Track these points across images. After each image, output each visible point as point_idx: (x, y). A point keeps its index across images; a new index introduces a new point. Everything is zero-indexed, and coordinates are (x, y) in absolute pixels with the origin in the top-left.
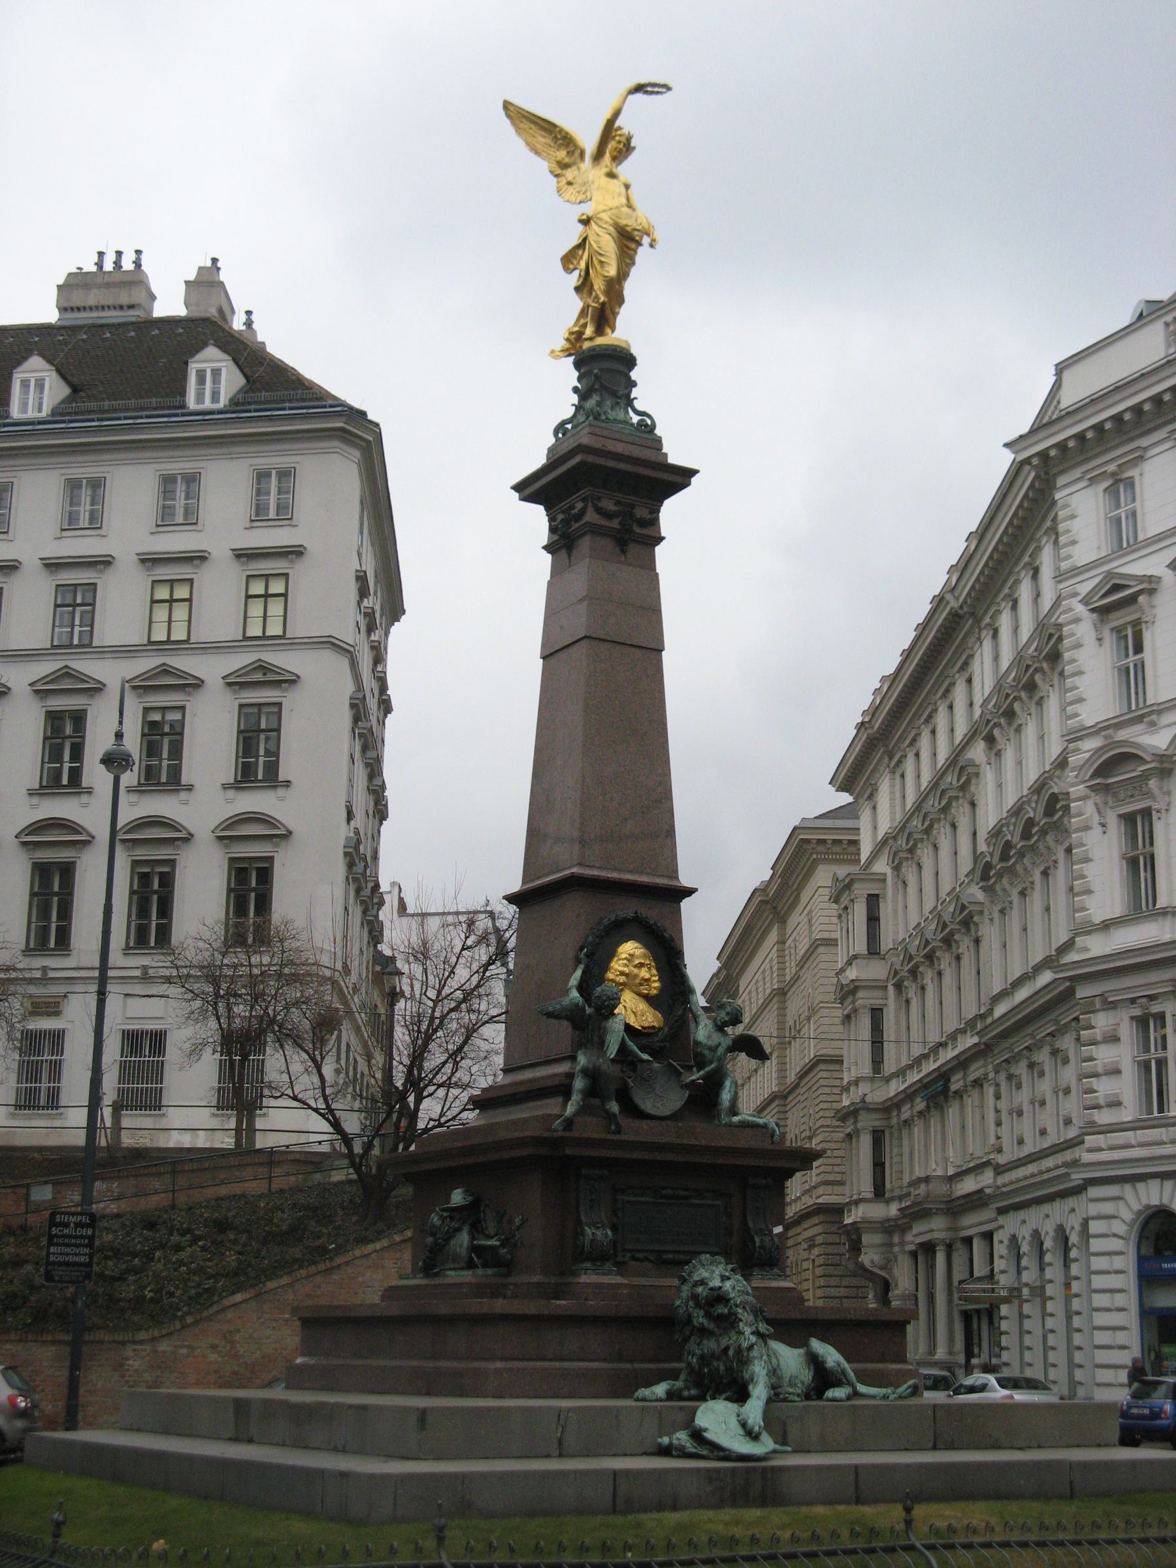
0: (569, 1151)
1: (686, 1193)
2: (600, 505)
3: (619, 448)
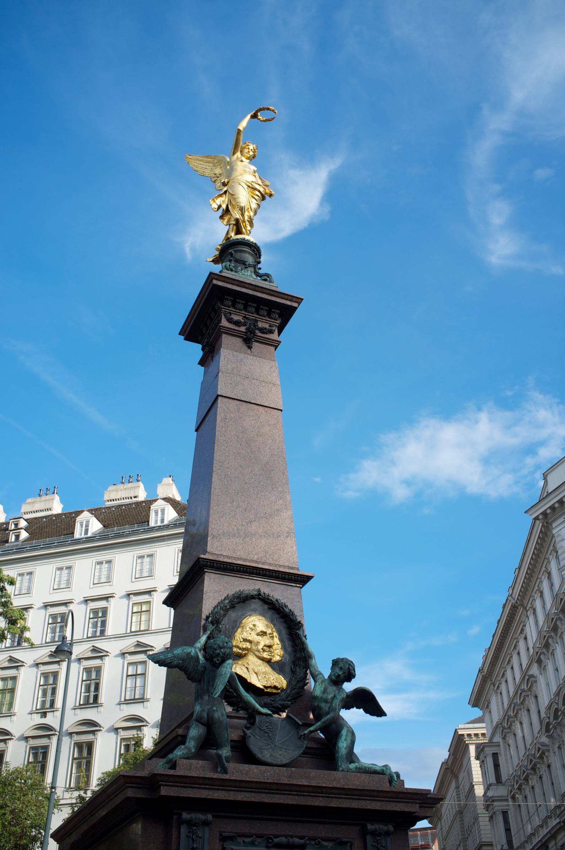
0: (164, 791)
1: (302, 841)
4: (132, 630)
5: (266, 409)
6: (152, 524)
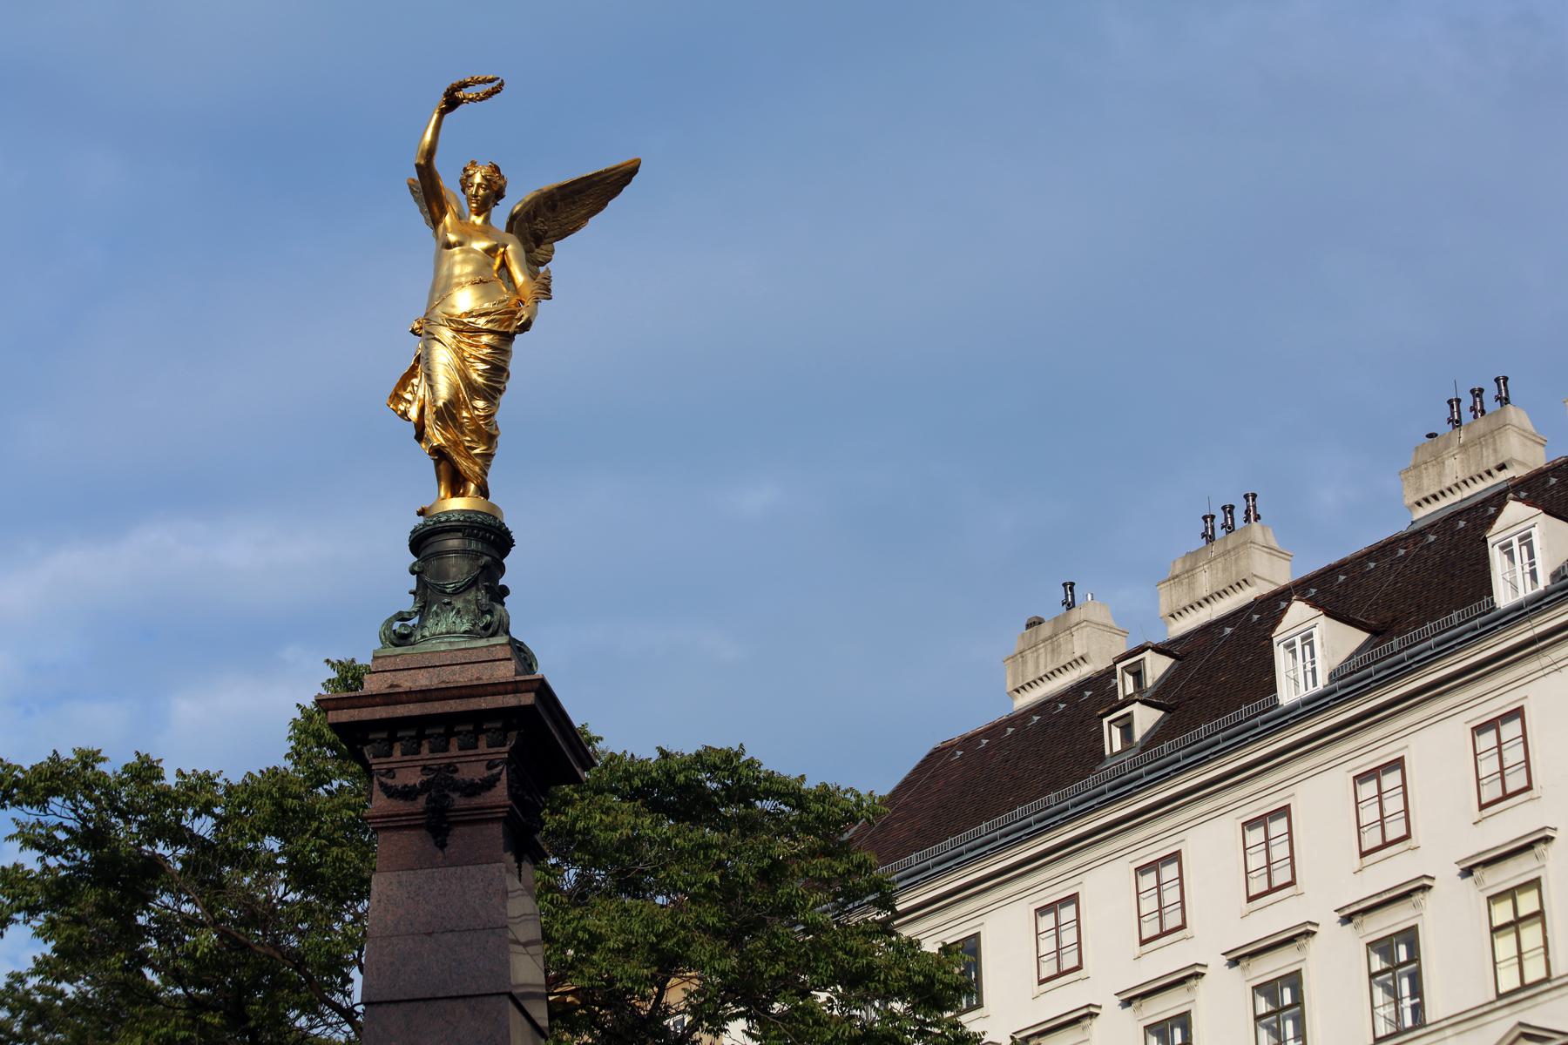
2: (390, 782)
3: (423, 680)
4: (1502, 990)
5: (473, 1001)
6: (1504, 598)
